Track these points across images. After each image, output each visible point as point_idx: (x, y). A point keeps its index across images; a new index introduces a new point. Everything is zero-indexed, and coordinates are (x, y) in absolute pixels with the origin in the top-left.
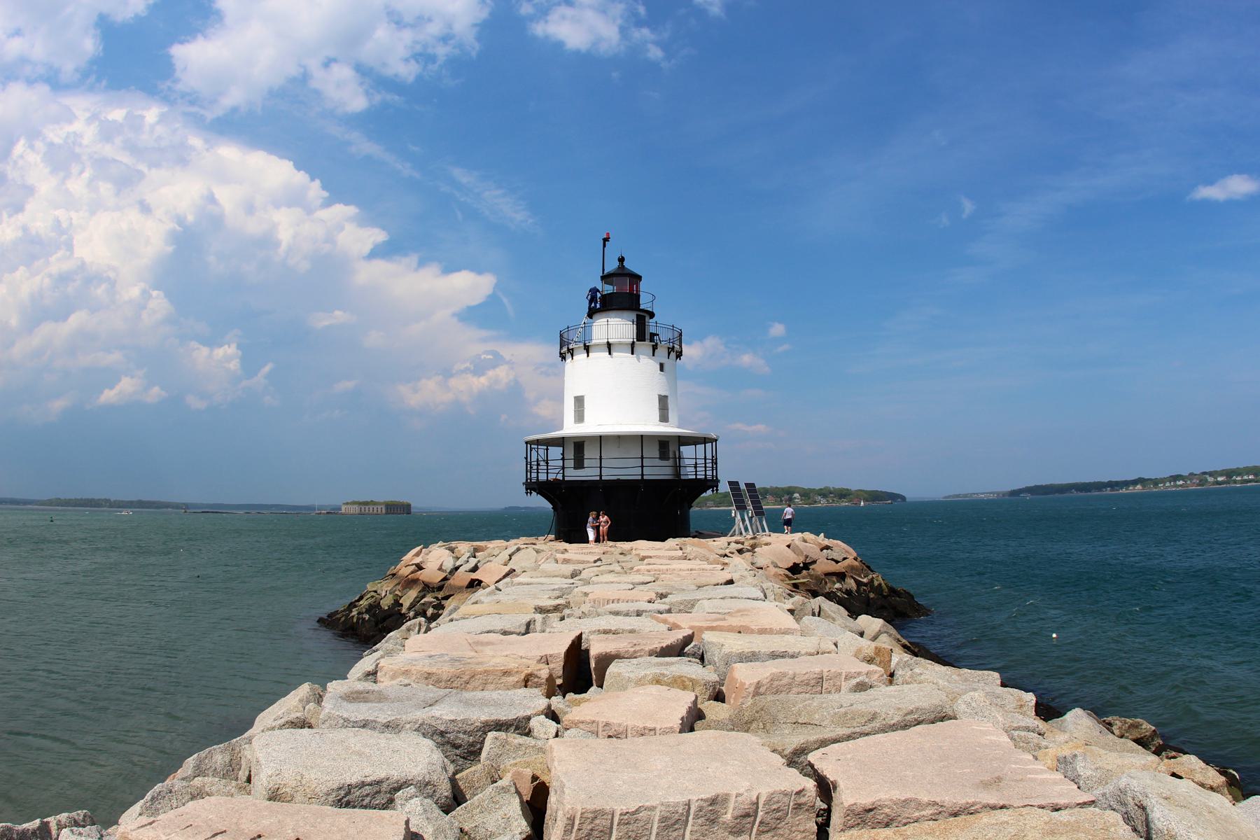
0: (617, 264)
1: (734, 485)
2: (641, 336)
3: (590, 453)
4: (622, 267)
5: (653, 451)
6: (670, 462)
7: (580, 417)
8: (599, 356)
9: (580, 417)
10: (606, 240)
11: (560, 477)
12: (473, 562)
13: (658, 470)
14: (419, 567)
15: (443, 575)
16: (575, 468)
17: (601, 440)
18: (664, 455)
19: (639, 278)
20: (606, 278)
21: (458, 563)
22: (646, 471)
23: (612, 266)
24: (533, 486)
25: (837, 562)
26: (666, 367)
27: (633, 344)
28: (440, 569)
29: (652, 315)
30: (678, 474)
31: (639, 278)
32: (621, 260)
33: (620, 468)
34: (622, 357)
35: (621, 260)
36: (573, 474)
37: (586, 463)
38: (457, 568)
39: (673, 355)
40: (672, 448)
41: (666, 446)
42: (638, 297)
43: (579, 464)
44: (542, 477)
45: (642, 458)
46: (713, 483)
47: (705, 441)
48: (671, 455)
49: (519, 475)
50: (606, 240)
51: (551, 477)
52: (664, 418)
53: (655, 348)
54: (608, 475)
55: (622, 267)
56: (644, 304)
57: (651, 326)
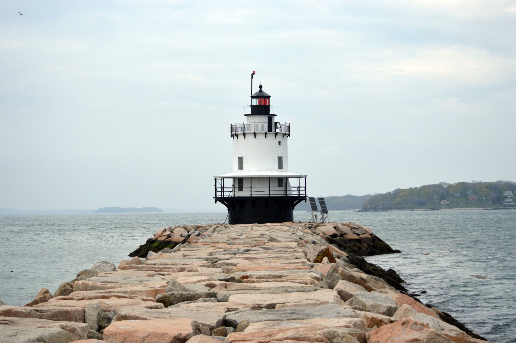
0: (259, 89)
2: (270, 130)
3: (246, 184)
4: (261, 91)
6: (283, 189)
7: (241, 167)
8: (250, 138)
9: (241, 167)
11: (232, 194)
12: (197, 232)
13: (277, 192)
14: (169, 236)
15: (183, 238)
17: (251, 179)
18: (280, 185)
19: (269, 97)
20: (253, 97)
21: (189, 233)
23: (256, 90)
26: (282, 143)
27: (266, 134)
28: (181, 236)
30: (287, 194)
31: (269, 97)
32: (261, 87)
34: (261, 138)
35: (261, 87)
36: (239, 194)
37: (244, 189)
38: (189, 236)
40: (284, 181)
42: (269, 107)
43: (241, 189)
44: (226, 195)
45: (270, 187)
50: (254, 73)
52: (280, 167)
53: (276, 134)
54: (255, 194)
55: (261, 91)
57: (275, 119)
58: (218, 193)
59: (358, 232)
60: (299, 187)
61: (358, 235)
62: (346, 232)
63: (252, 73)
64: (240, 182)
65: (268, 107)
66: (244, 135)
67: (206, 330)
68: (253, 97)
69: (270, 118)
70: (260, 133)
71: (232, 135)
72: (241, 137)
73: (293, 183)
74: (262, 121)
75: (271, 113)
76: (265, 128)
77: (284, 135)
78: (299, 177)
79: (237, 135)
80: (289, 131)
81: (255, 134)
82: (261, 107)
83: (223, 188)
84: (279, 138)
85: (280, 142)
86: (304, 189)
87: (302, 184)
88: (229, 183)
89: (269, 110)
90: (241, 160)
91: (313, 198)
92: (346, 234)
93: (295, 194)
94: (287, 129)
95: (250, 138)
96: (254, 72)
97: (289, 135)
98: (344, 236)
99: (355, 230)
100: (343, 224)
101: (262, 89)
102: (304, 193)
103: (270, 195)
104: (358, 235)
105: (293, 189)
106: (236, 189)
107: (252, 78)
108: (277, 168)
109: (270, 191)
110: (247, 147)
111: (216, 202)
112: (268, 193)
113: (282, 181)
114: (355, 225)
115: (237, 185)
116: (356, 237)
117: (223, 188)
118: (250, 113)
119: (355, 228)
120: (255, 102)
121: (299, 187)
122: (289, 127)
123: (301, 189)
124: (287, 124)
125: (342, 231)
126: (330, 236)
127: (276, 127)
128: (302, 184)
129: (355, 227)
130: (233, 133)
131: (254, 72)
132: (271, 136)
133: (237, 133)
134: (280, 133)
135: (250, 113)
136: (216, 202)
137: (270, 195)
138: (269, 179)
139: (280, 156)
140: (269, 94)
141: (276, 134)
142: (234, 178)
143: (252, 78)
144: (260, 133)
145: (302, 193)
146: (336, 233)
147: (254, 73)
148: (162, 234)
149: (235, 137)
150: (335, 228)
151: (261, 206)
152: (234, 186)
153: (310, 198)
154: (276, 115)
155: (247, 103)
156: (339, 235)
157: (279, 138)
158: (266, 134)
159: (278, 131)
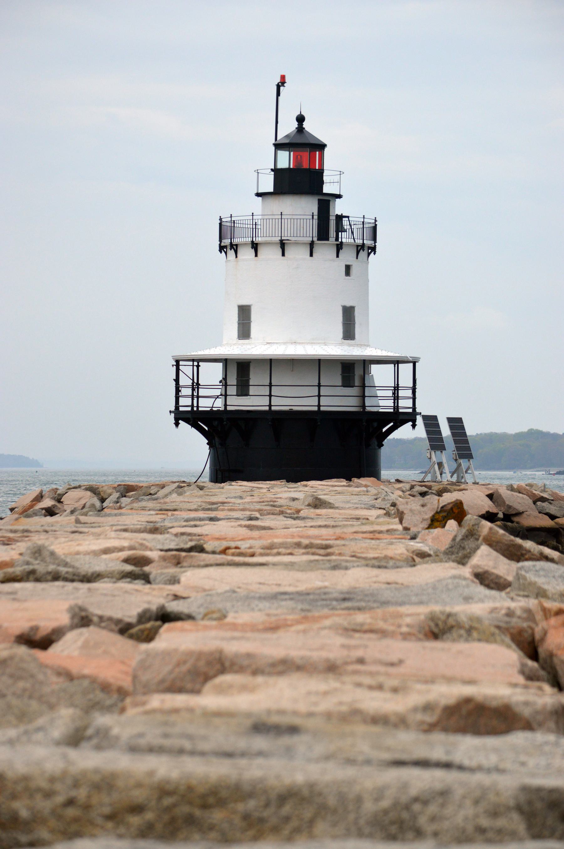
0: (295, 124)
1: (431, 422)
2: (323, 234)
3: (256, 378)
4: (300, 129)
7: (244, 332)
8: (270, 254)
9: (244, 332)
11: (219, 404)
17: (271, 364)
19: (321, 147)
20: (278, 146)
22: (323, 401)
23: (288, 127)
26: (353, 271)
27: (312, 245)
30: (364, 406)
32: (301, 119)
33: (293, 397)
34: (297, 254)
35: (301, 119)
37: (252, 390)
39: (363, 254)
40: (358, 372)
42: (321, 172)
43: (243, 389)
44: (205, 404)
48: (357, 383)
50: (282, 82)
52: (349, 333)
53: (339, 247)
54: (281, 404)
55: (300, 129)
57: (339, 207)
58: (182, 401)
59: (552, 509)
60: (396, 388)
61: (553, 517)
62: (521, 509)
63: (278, 80)
64: (241, 371)
66: (255, 246)
68: (278, 146)
69: (325, 203)
70: (296, 243)
71: (222, 248)
72: (246, 253)
73: (381, 376)
74: (300, 210)
75: (327, 189)
76: (310, 229)
77: (360, 248)
78: (396, 362)
79: (235, 247)
80: (374, 239)
81: (283, 245)
82: (301, 172)
83: (196, 386)
84: (348, 256)
85: (348, 269)
86: (409, 393)
87: (406, 380)
88: (212, 374)
89: (322, 183)
90: (244, 312)
91: (435, 418)
92: (519, 514)
93: (385, 405)
94: (367, 233)
95: (270, 254)
96: (283, 77)
97: (373, 249)
98: (516, 519)
99: (545, 504)
100: (511, 488)
101: (305, 125)
102: (409, 403)
104: (553, 517)
105: (379, 393)
106: (232, 390)
107: (278, 94)
108: (341, 335)
109: (319, 396)
110: (260, 277)
111: (177, 424)
112: (315, 401)
113: (352, 372)
114: (544, 491)
115: (232, 380)
116: (547, 522)
117: (196, 386)
118: (271, 190)
119: (543, 499)
120: (285, 160)
121: (396, 388)
122: (375, 228)
123: (401, 393)
124: (370, 220)
125: (510, 507)
127: (340, 228)
128: (406, 380)
129: (545, 495)
130: (226, 242)
131: (283, 77)
132: (325, 252)
133: (236, 241)
134: (349, 245)
135: (271, 190)
136: (177, 424)
138: (319, 364)
139: (348, 304)
140: (323, 139)
141: (339, 247)
142: (226, 362)
143: (278, 94)
144: (296, 243)
145: (405, 404)
146: (494, 510)
147: (282, 82)
148: (31, 506)
149: (231, 253)
150: (490, 496)
151: (294, 435)
152: (224, 382)
154: (339, 196)
155: (263, 162)
156: (501, 515)
157: (348, 256)
158: (312, 245)
159: (345, 238)
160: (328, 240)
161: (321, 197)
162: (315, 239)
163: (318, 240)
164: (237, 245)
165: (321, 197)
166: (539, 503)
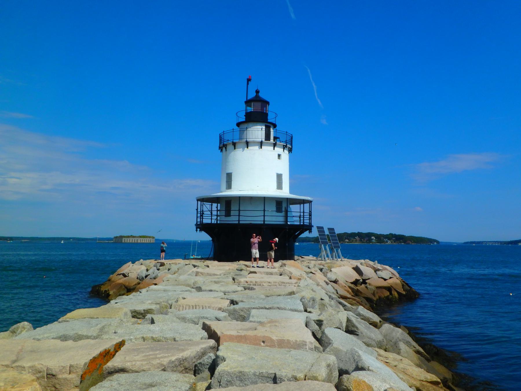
0: (255, 94)
3: (234, 207)
5: (271, 208)
10: (249, 80)
13: (274, 218)
16: (226, 216)
17: (240, 199)
20: (248, 102)
22: (267, 219)
23: (252, 95)
24: (202, 227)
25: (385, 280)
29: (275, 126)
31: (268, 103)
32: (257, 92)
35: (257, 92)
40: (284, 205)
41: (280, 204)
43: (228, 214)
45: (264, 211)
46: (309, 228)
47: (303, 202)
48: (283, 209)
49: (193, 220)
51: (213, 222)
52: (280, 186)
56: (271, 118)
65: (266, 115)
67: (225, 317)
85: (279, 156)
91: (322, 228)
102: (308, 221)
103: (264, 221)
107: (248, 84)
108: (276, 187)
109: (264, 216)
112: (262, 218)
118: (244, 120)
120: (250, 109)
126: (352, 283)
128: (307, 210)
135: (244, 120)
137: (264, 221)
139: (279, 173)
143: (248, 84)
153: (318, 227)
160: (270, 140)
161: (267, 124)
162: (264, 140)
163: (265, 140)
164: (226, 145)
165: (267, 124)
166: (378, 272)
